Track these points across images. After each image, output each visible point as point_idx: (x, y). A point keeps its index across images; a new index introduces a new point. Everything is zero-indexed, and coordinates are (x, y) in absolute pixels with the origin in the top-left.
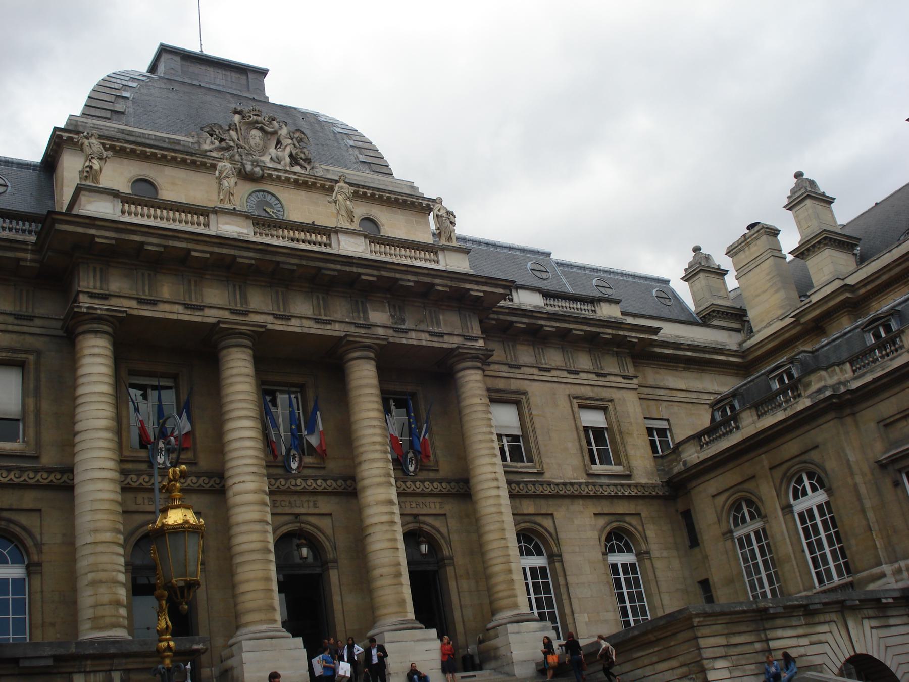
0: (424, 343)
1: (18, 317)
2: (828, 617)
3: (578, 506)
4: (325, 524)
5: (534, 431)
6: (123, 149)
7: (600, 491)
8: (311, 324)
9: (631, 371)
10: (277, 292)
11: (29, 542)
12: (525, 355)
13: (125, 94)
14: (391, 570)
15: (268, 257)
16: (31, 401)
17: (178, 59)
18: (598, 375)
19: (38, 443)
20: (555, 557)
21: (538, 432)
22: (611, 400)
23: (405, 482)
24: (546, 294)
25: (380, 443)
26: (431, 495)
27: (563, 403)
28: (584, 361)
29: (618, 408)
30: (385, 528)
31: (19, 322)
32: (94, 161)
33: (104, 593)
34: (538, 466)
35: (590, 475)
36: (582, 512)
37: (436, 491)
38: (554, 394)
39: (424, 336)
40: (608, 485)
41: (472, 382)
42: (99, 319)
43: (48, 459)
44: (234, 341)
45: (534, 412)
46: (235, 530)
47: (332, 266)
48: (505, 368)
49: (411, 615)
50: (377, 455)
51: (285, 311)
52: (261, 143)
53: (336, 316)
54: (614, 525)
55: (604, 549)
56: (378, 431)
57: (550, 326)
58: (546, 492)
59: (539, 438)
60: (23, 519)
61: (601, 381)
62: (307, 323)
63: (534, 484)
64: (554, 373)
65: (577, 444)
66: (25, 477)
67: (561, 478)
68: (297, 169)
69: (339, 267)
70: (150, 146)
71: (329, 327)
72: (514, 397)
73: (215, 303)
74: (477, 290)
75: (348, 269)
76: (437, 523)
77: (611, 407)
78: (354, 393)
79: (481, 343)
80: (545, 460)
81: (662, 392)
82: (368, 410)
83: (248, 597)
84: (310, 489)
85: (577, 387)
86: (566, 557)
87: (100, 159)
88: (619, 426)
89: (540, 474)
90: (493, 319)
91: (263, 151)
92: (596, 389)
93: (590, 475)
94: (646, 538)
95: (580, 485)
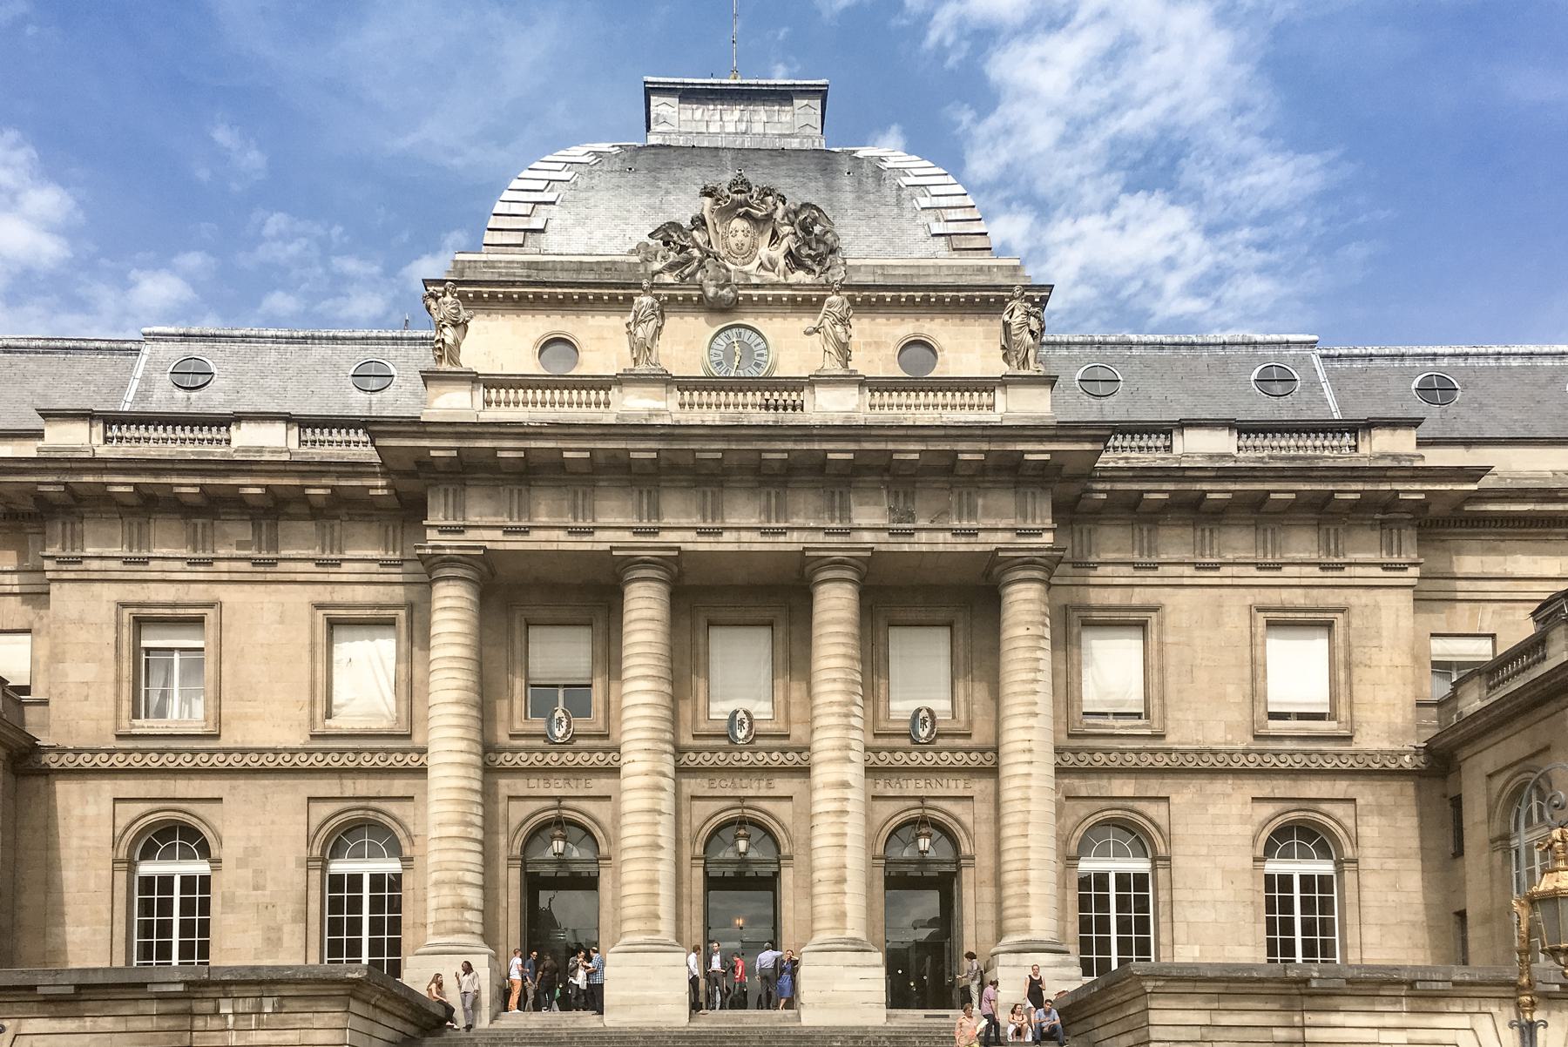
4: (783, 811)
5: (1162, 670)
7: (1271, 762)
14: (832, 874)
16: (403, 667)
21: (1171, 672)
23: (907, 751)
25: (840, 703)
29: (1355, 622)
30: (832, 819)
31: (386, 570)
34: (1156, 725)
35: (1255, 737)
36: (1229, 795)
37: (958, 765)
38: (1220, 606)
40: (1292, 753)
43: (417, 740)
45: (1169, 639)
46: (624, 821)
49: (855, 928)
50: (833, 720)
52: (747, 241)
56: (839, 686)
58: (1161, 765)
59: (1171, 680)
63: (1138, 752)
64: (1225, 571)
65: (1248, 687)
66: (391, 759)
67: (1198, 742)
68: (800, 276)
72: (1134, 616)
78: (816, 632)
80: (1172, 714)
82: (829, 657)
83: (627, 902)
84: (761, 765)
85: (1269, 591)
88: (1349, 654)
90: (1101, 491)
92: (1315, 592)
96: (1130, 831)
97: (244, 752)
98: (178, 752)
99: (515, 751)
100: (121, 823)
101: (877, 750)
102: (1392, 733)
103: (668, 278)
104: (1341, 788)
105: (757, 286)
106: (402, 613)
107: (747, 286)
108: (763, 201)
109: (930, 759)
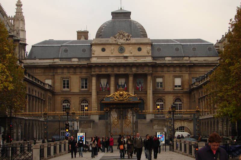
0: (141, 73)
1: (86, 73)
2: (178, 121)
3: (170, 95)
9: (188, 70)
11: (88, 101)
12: (165, 69)
13: (102, 31)
17: (114, 14)
18: (180, 72)
19: (89, 89)
20: (164, 103)
22: (182, 76)
24: (172, 57)
26: (143, 94)
27: (171, 77)
28: (178, 69)
33: (94, 109)
39: (141, 72)
40: (177, 91)
41: (149, 78)
42: (94, 75)
44: (112, 76)
48: (160, 72)
54: (177, 98)
55: (174, 101)
57: (168, 65)
60: (88, 98)
61: (181, 73)
62: (122, 72)
64: (171, 72)
68: (128, 41)
73: (109, 71)
74: (150, 64)
76: (144, 98)
77: (182, 77)
79: (151, 72)
80: (165, 87)
81: (198, 72)
86: (166, 103)
89: (164, 90)
91: (122, 39)
93: (174, 90)
94: (183, 100)
95: (171, 92)
96: (161, 100)
97: (73, 93)
98: (67, 93)
99: (100, 92)
100: (61, 100)
101: (136, 92)
102: (187, 89)
103: (114, 42)
104: (182, 95)
106: (88, 78)
109: (141, 93)
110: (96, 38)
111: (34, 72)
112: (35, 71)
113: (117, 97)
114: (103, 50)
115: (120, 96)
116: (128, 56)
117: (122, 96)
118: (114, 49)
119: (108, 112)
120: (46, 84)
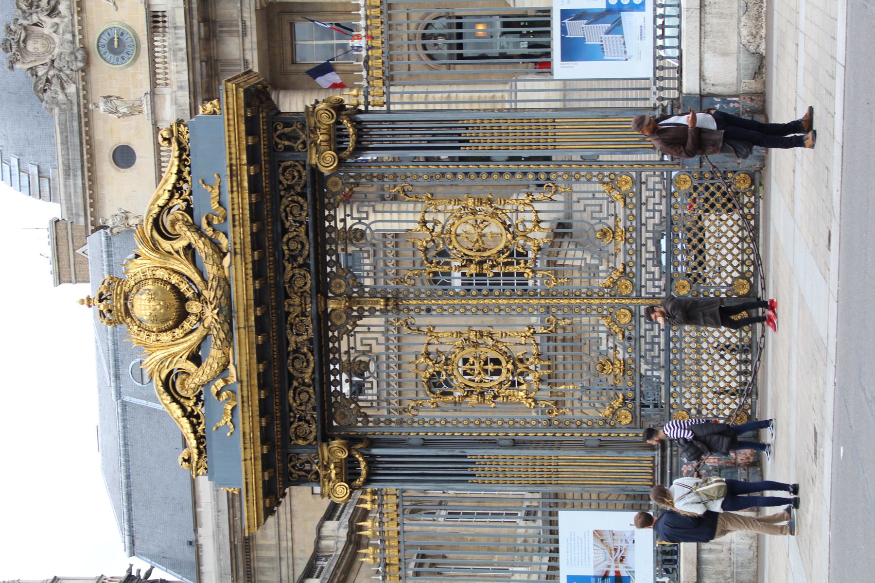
4: (416, 17)
6: (90, 180)
8: (248, 39)
10: (223, 71)
13: (14, 162)
15: (199, 89)
32: (131, 224)
47: (195, 28)
51: (240, 65)
52: (40, 41)
53: (235, 15)
62: (248, 45)
69: (195, 22)
70: (82, 156)
71: (248, 23)
75: (195, 13)
87: (127, 218)
91: (47, 38)
103: (71, 89)
105: (74, 36)
107: (73, 42)
108: (15, 32)
110: (55, 201)
111: (273, 554)
112: (268, 548)
113: (196, 358)
114: (124, 157)
115: (183, 315)
116: (148, 6)
117: (182, 299)
118: (108, 98)
119: (371, 461)
120: (319, 538)
